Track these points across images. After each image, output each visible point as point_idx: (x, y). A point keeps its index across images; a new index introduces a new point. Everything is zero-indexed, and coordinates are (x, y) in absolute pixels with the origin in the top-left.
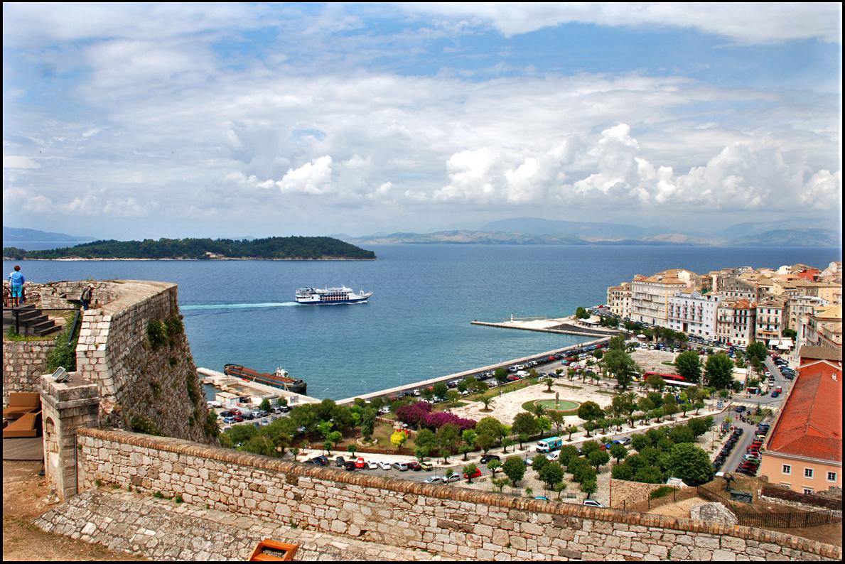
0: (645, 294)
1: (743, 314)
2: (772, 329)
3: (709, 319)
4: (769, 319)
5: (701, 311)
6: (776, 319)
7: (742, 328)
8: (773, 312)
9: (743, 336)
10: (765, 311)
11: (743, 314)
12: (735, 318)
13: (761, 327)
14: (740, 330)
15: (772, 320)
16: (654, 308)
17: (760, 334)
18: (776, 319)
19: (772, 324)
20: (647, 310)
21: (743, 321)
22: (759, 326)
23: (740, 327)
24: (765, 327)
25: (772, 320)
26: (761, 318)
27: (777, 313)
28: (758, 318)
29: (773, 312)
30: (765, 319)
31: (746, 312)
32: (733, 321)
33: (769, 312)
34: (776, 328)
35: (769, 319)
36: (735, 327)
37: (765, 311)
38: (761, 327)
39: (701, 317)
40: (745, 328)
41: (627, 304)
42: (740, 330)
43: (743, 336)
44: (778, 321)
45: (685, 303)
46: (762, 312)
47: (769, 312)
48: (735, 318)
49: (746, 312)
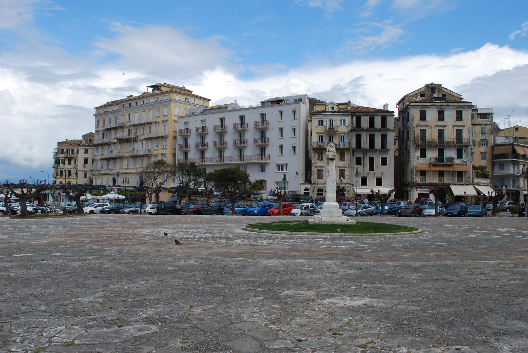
0: (122, 127)
2: (451, 159)
3: (287, 149)
4: (441, 133)
5: (262, 132)
7: (377, 161)
8: (450, 115)
9: (379, 182)
10: (432, 115)
11: (378, 124)
13: (423, 155)
14: (372, 168)
15: (450, 135)
16: (142, 153)
17: (423, 173)
18: (459, 133)
19: (450, 146)
20: (125, 162)
21: (378, 144)
22: (418, 153)
23: (372, 160)
24: (432, 155)
25: (450, 135)
26: (423, 132)
29: (450, 115)
30: (432, 135)
32: (354, 145)
33: (441, 116)
34: (460, 156)
35: (441, 133)
36: (359, 162)
38: (423, 155)
39: (262, 150)
40: (384, 162)
41: (86, 161)
42: (372, 168)
43: (379, 182)
46: (423, 117)
47: (441, 116)
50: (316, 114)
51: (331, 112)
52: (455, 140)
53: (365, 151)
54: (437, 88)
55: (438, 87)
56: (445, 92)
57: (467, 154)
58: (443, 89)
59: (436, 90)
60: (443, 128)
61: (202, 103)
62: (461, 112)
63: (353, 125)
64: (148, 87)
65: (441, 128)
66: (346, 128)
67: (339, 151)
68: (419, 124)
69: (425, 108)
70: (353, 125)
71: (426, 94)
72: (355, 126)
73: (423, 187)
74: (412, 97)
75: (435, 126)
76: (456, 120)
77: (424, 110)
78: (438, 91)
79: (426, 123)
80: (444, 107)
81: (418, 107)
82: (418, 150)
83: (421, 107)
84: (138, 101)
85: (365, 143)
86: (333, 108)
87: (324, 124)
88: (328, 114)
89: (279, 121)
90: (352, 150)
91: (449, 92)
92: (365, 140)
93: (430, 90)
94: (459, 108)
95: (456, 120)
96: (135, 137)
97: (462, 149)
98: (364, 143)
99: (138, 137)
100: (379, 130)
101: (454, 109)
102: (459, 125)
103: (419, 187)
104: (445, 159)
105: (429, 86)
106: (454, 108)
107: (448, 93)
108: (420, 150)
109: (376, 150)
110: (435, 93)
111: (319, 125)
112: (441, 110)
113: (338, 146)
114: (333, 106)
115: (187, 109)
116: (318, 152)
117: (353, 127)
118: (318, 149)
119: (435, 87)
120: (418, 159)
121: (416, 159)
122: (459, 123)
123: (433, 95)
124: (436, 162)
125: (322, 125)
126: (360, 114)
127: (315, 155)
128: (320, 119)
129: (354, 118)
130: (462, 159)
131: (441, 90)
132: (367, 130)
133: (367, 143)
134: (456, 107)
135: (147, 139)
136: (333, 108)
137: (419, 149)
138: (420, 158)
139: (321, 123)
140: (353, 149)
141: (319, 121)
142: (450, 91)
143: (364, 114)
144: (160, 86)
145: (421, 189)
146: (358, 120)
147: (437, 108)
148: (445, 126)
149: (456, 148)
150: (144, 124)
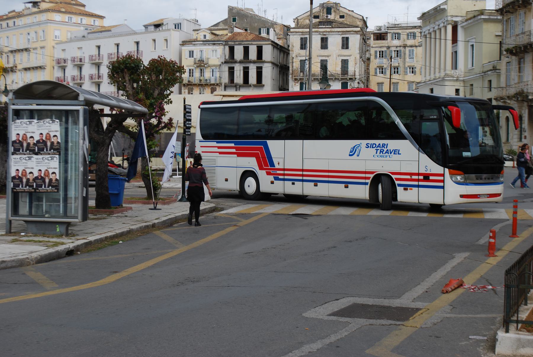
1: (253, 55)
6: (345, 63)
8: (335, 41)
11: (253, 55)
12: (231, 71)
18: (345, 63)
25: (334, 68)
27: (345, 44)
28: (295, 65)
29: (335, 41)
31: (260, 50)
32: (225, 79)
37: (316, 40)
44: (351, 68)
45: (95, 52)
48: (231, 71)
49: (260, 50)
50: (186, 44)
51: (203, 41)
52: (340, 72)
53: (238, 86)
54: (333, 7)
55: (335, 6)
56: (343, 12)
58: (341, 9)
61: (93, 21)
62: (347, 39)
63: (225, 56)
64: (25, 3)
65: (324, 58)
66: (218, 59)
67: (210, 87)
68: (300, 54)
70: (225, 56)
71: (321, 15)
72: (227, 57)
74: (304, 20)
75: (318, 56)
76: (342, 49)
77: (305, 38)
80: (328, 33)
81: (298, 33)
82: (297, 84)
83: (301, 33)
84: (15, 20)
85: (239, 78)
86: (205, 36)
87: (195, 56)
88: (198, 44)
89: (151, 52)
90: (223, 85)
91: (347, 12)
92: (238, 74)
93: (325, 10)
94: (345, 34)
95: (342, 49)
96: (13, 67)
98: (237, 77)
99: (16, 67)
100: (254, 62)
101: (339, 36)
102: (345, 54)
105: (325, 5)
106: (339, 34)
107: (347, 14)
109: (250, 86)
110: (331, 14)
111: (190, 57)
112: (325, 36)
113: (208, 81)
114: (205, 34)
115: (70, 32)
116: (188, 88)
117: (225, 59)
118: (188, 85)
119: (332, 6)
122: (345, 52)
123: (327, 17)
125: (193, 57)
126: (233, 43)
127: (185, 92)
128: (190, 50)
129: (227, 48)
131: (338, 10)
132: (241, 62)
133: (240, 78)
134: (341, 33)
135: (26, 69)
136: (205, 36)
137: (299, 83)
139: (191, 54)
140: (225, 84)
141: (190, 52)
143: (237, 43)
144: (40, 2)
146: (232, 50)
147: (320, 34)
148: (328, 56)
149: (341, 82)
150: (22, 50)
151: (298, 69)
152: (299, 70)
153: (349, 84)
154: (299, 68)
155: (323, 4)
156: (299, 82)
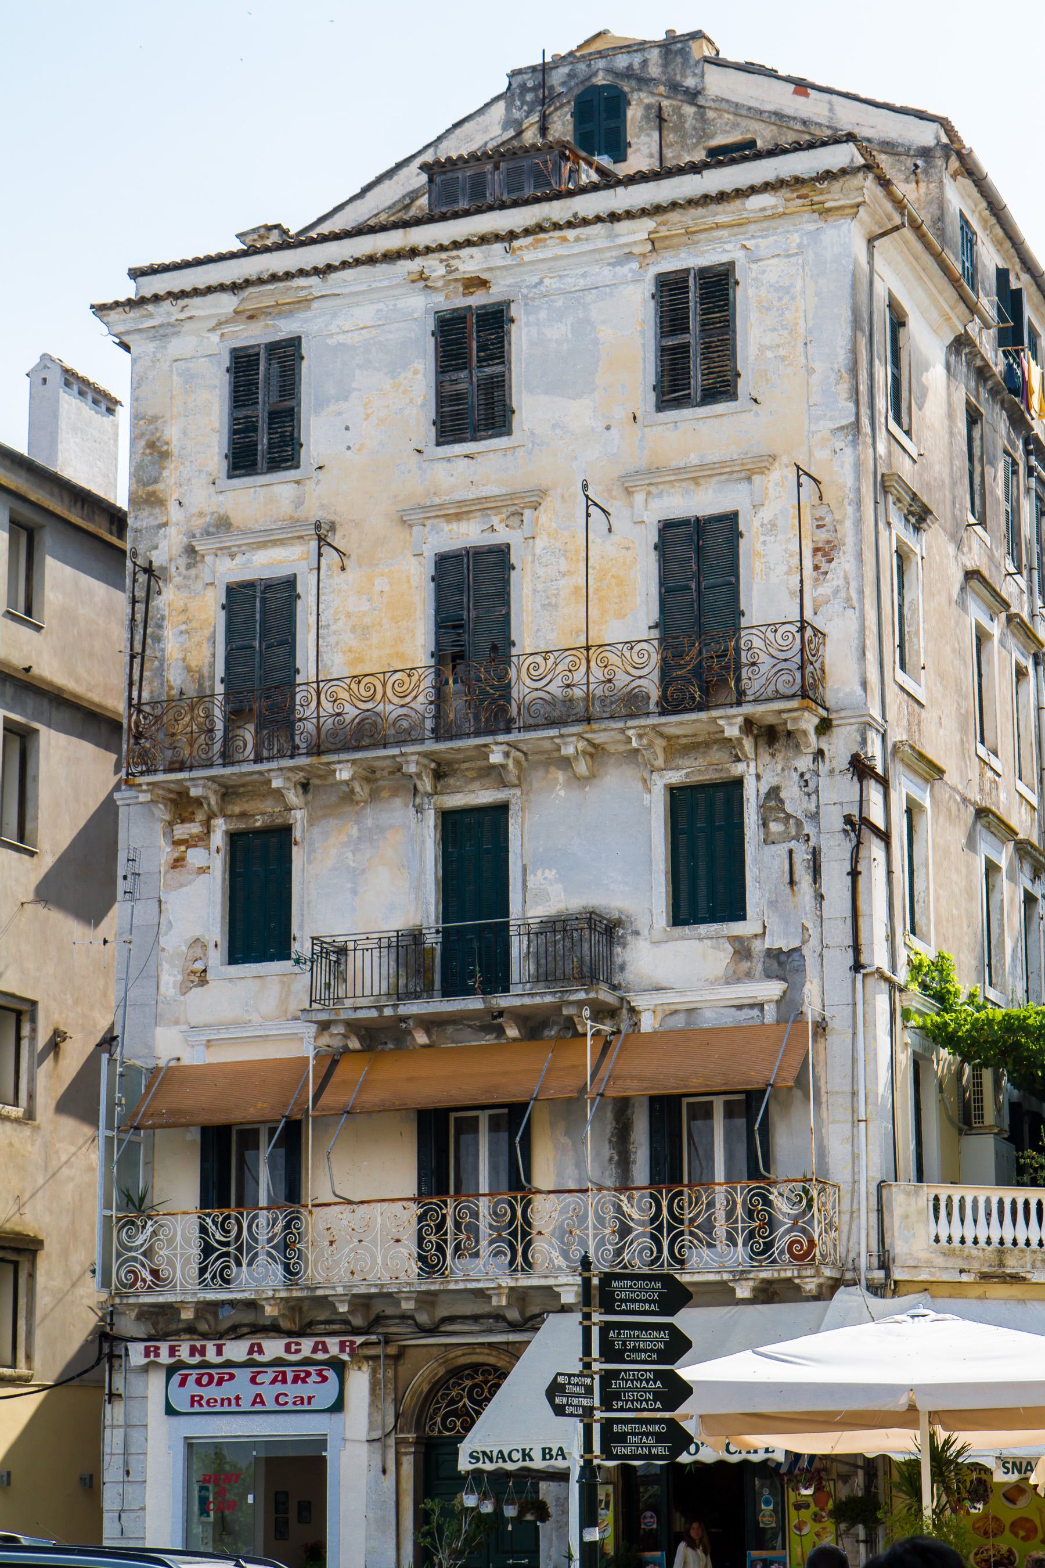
54: (643, 81)
56: (737, 109)
57: (802, 855)
59: (634, 113)
60: (502, 535)
69: (280, 310)
73: (236, 1350)
78: (660, 120)
79: (299, 502)
82: (196, 857)
91: (783, 99)
97: (738, 783)
103: (184, 1353)
104: (518, 947)
105: (556, 78)
108: (218, 864)
112: (478, 299)
119: (628, 74)
120: (202, 978)
121: (170, 979)
124: (400, 996)
130: (737, 928)
131: (693, 96)
137: (218, 839)
138: (216, 957)
142: (802, 86)
145: (228, 1390)
149: (660, 782)
151: (204, 697)
152: (220, 688)
153: (751, 792)
154: (220, 671)
155: (543, 70)
156: (220, 828)
